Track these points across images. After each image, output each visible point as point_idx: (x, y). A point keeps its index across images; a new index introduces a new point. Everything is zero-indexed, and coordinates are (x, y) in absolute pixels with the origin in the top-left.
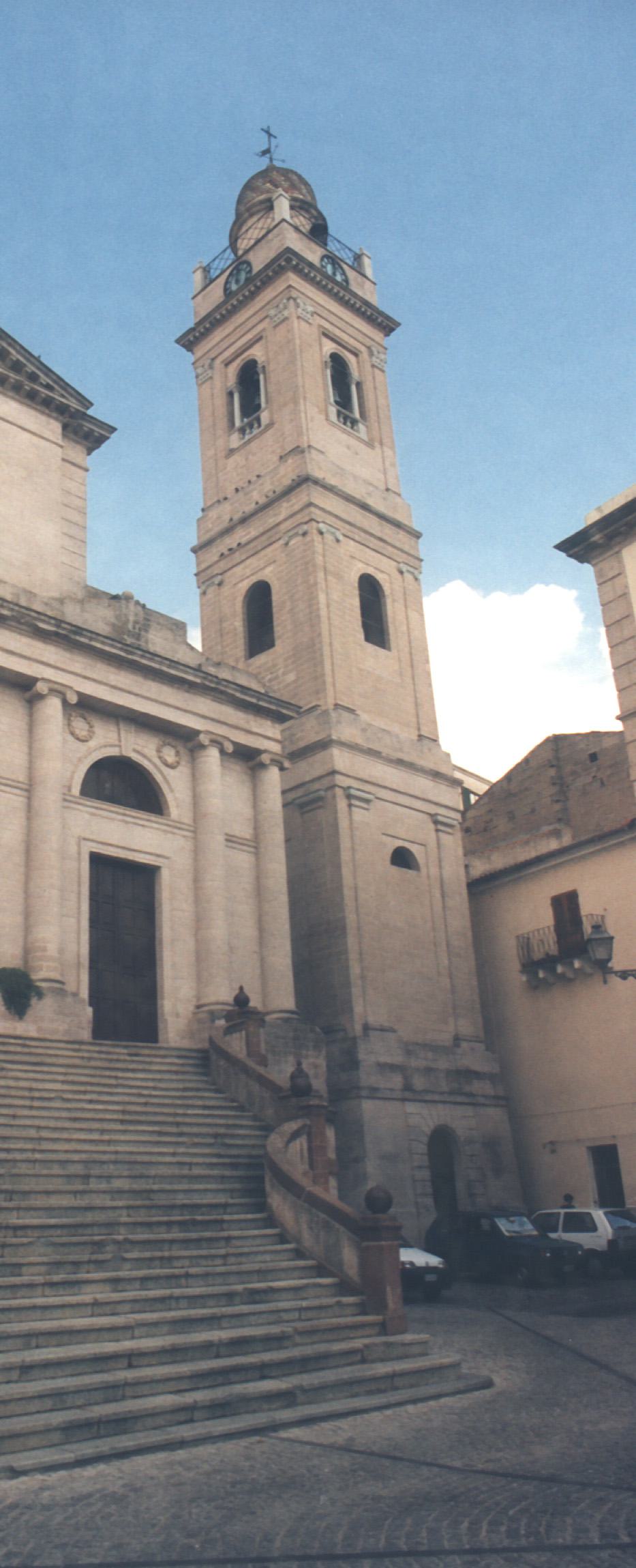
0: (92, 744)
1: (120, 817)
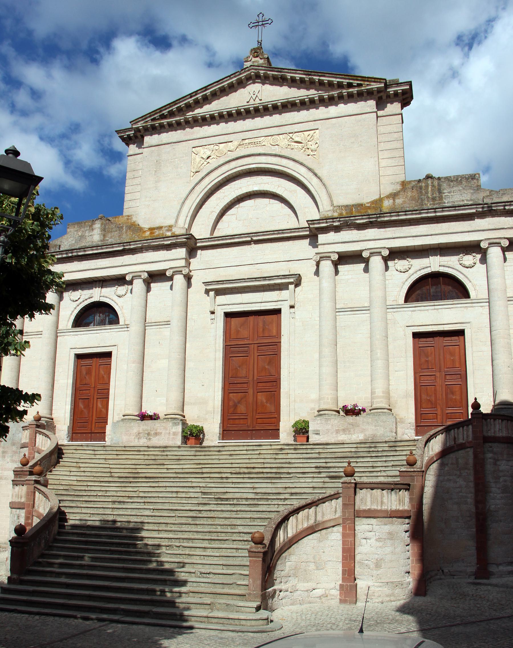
0: (411, 271)
1: (433, 307)
